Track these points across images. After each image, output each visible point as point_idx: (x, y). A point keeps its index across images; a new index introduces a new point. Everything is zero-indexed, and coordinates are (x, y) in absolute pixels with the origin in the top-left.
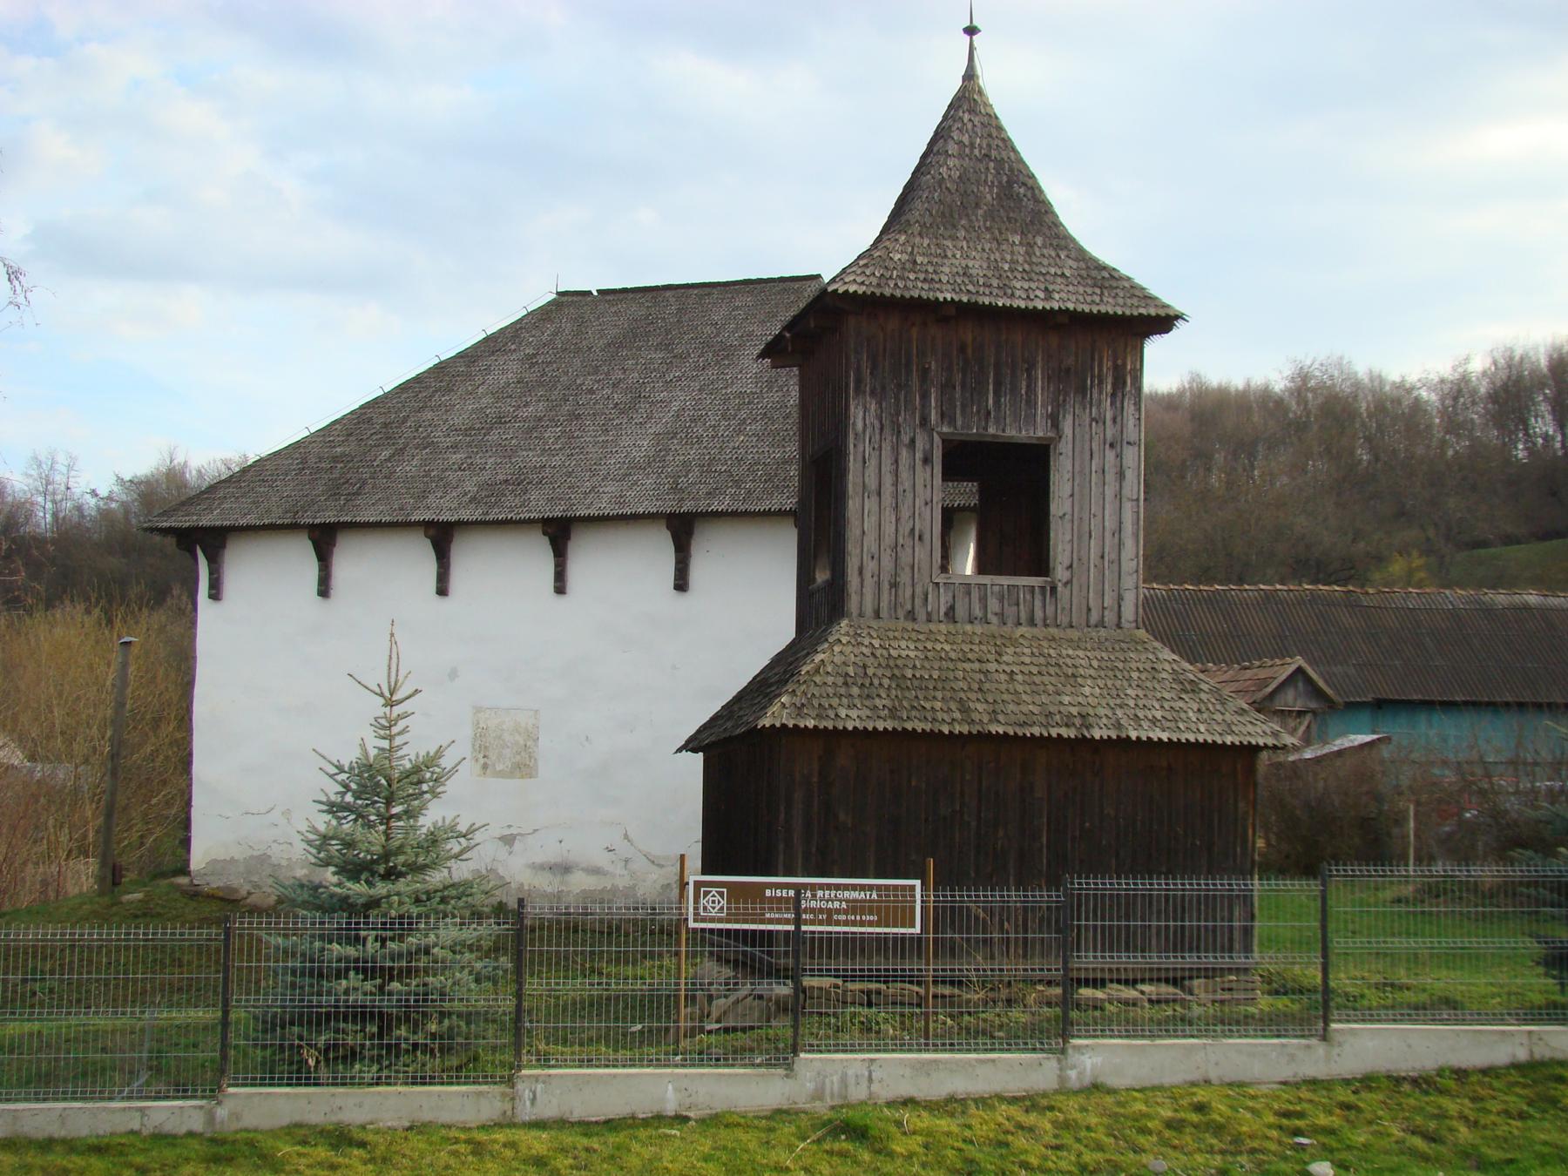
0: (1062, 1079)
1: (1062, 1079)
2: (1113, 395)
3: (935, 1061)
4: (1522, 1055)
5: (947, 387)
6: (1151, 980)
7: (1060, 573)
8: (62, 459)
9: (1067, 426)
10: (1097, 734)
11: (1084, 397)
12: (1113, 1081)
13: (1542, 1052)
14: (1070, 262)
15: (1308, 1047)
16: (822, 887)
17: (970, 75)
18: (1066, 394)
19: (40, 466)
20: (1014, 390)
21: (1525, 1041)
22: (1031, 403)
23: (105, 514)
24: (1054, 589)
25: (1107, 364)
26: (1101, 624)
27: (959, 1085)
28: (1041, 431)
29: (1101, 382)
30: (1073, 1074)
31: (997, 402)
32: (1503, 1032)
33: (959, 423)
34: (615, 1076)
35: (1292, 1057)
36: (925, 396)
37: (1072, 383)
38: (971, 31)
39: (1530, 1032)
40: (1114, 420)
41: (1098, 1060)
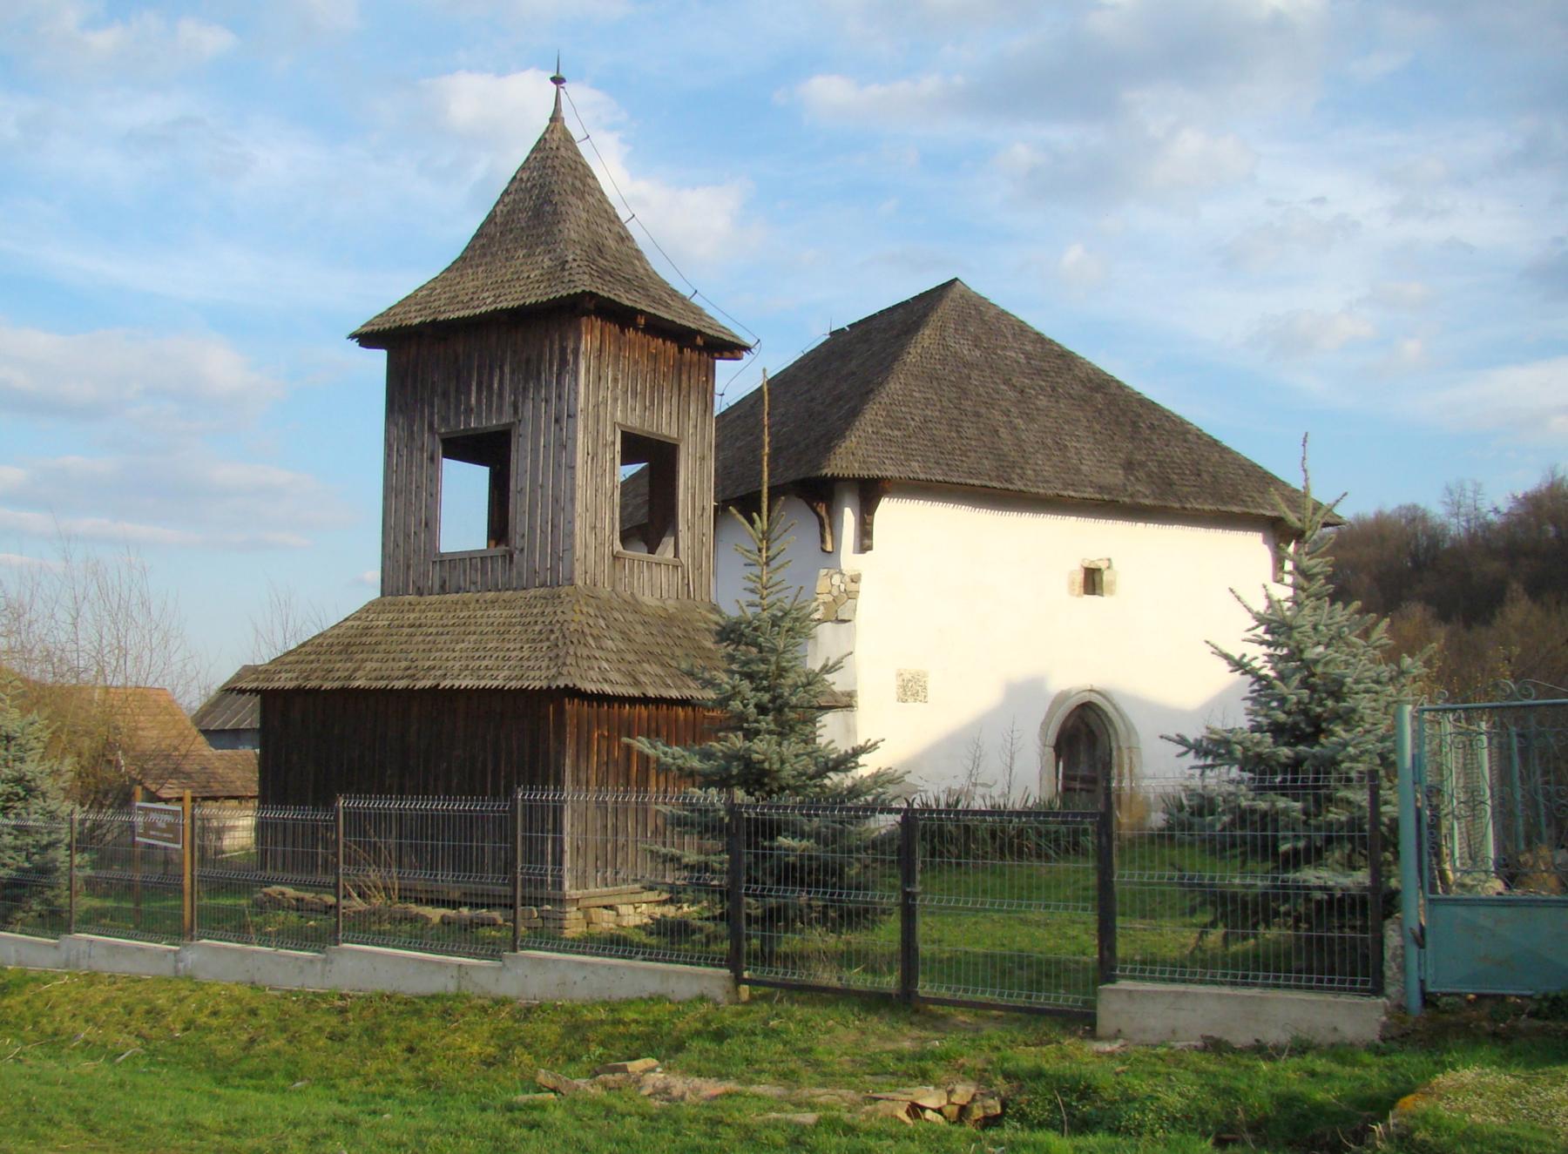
0: (176, 970)
1: (176, 970)
2: (559, 375)
3: (117, 946)
4: (452, 987)
5: (445, 395)
6: (488, 906)
7: (517, 541)
8: (1469, 486)
9: (528, 411)
10: (420, 685)
11: (539, 379)
12: (202, 976)
13: (468, 988)
14: (547, 263)
15: (311, 961)
16: (154, 810)
17: (556, 118)
18: (526, 382)
19: (1451, 493)
20: (490, 387)
21: (455, 973)
22: (501, 396)
23: (1507, 526)
24: (511, 556)
25: (556, 347)
26: (543, 585)
27: (124, 966)
28: (506, 420)
29: (551, 365)
30: (181, 965)
31: (479, 401)
32: (439, 963)
33: (452, 422)
34: (141, 949)
35: (302, 971)
36: (432, 406)
37: (530, 372)
38: (557, 81)
39: (460, 966)
40: (559, 397)
41: (195, 956)
